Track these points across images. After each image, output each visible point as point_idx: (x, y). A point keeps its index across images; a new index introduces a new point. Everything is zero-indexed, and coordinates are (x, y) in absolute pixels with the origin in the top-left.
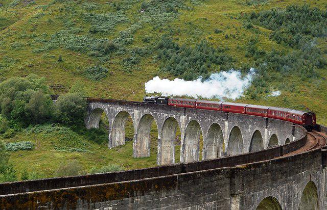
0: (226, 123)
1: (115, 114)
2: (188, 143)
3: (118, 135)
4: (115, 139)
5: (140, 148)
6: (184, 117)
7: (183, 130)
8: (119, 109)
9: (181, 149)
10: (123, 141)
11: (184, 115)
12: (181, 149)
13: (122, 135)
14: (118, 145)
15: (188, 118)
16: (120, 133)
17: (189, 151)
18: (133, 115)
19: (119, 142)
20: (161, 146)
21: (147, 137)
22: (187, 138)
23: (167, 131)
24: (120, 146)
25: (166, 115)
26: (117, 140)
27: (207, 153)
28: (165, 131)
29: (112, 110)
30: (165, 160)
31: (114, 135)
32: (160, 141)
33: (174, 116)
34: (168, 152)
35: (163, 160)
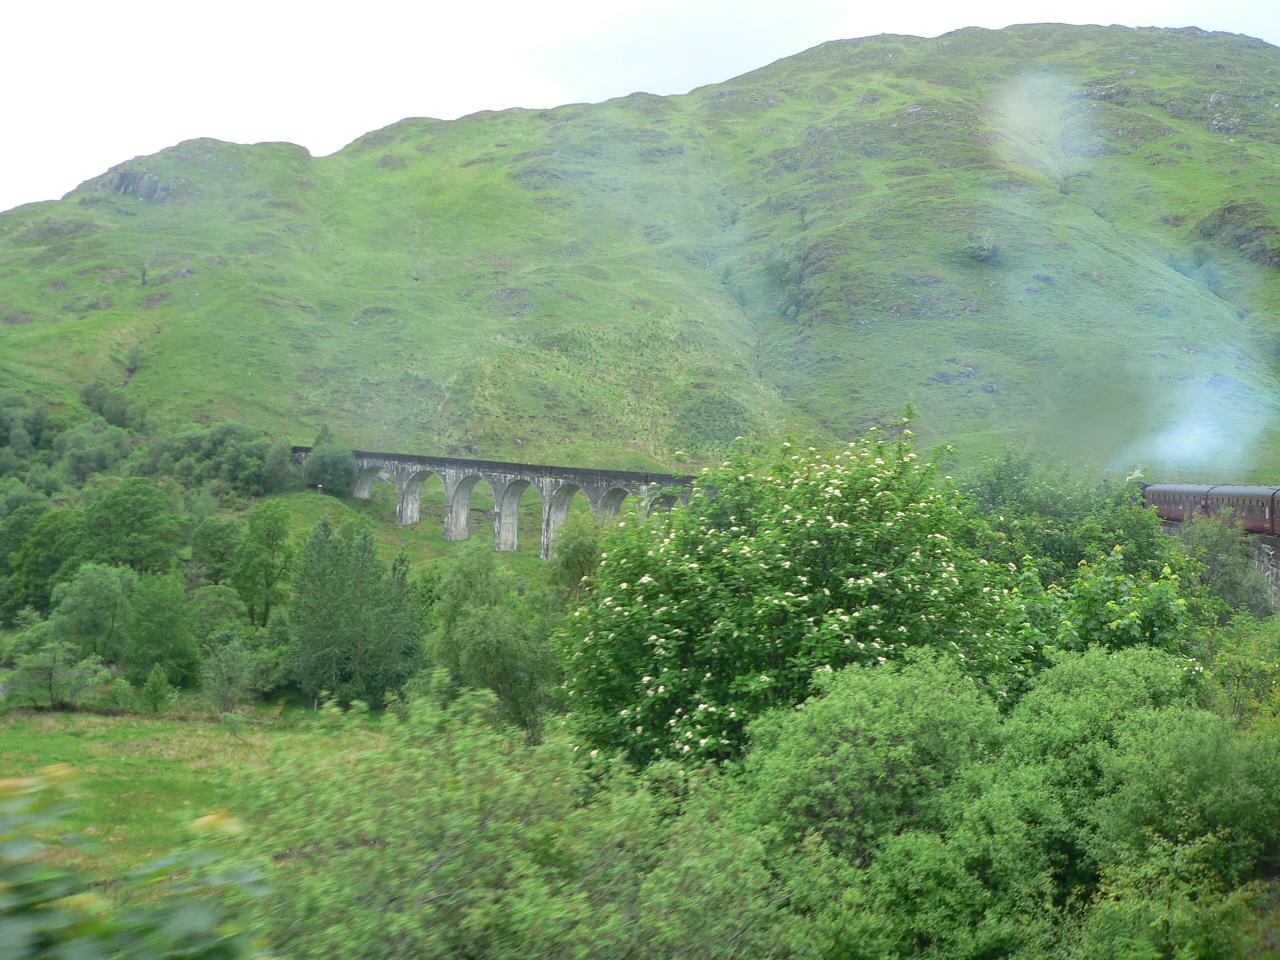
1: (409, 474)
2: (553, 518)
3: (410, 506)
6: (548, 480)
8: (418, 468)
9: (543, 526)
10: (416, 516)
12: (543, 526)
13: (416, 506)
14: (410, 522)
18: (444, 477)
20: (500, 522)
22: (553, 509)
24: (415, 524)
25: (509, 477)
28: (506, 500)
29: (403, 469)
32: (499, 515)
33: (527, 478)
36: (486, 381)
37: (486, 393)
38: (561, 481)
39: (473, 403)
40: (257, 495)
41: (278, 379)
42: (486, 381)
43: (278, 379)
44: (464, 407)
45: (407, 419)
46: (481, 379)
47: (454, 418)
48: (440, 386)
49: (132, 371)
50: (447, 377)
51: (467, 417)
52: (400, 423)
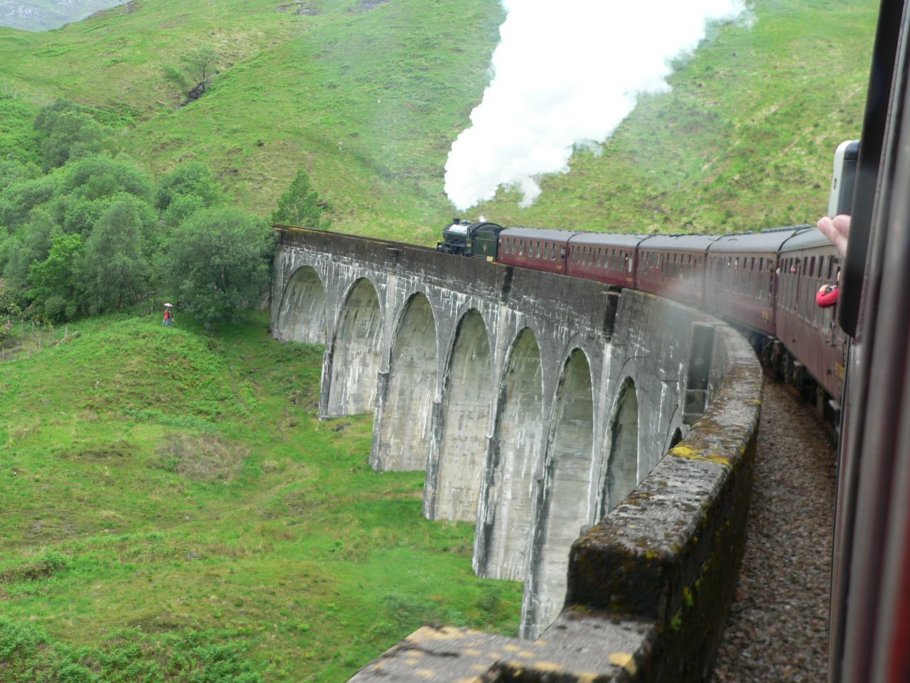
0: (608, 350)
3: (355, 368)
4: (344, 385)
5: (400, 431)
7: (498, 371)
8: (352, 270)
11: (504, 299)
14: (352, 409)
15: (514, 316)
16: (365, 365)
17: (517, 473)
18: (384, 292)
19: (358, 399)
21: (432, 387)
22: (513, 409)
23: (472, 370)
26: (351, 387)
27: (553, 507)
28: (462, 370)
29: (337, 274)
30: (457, 499)
31: (337, 365)
34: (473, 462)
35: (446, 493)
36: (834, 115)
37: (819, 140)
38: (518, 314)
39: (779, 158)
40: (60, 318)
41: (426, 111)
42: (834, 115)
43: (426, 111)
44: (755, 165)
45: (626, 189)
46: (826, 108)
47: (719, 188)
48: (731, 125)
49: (194, 95)
50: (759, 106)
51: (749, 186)
52: (610, 196)
